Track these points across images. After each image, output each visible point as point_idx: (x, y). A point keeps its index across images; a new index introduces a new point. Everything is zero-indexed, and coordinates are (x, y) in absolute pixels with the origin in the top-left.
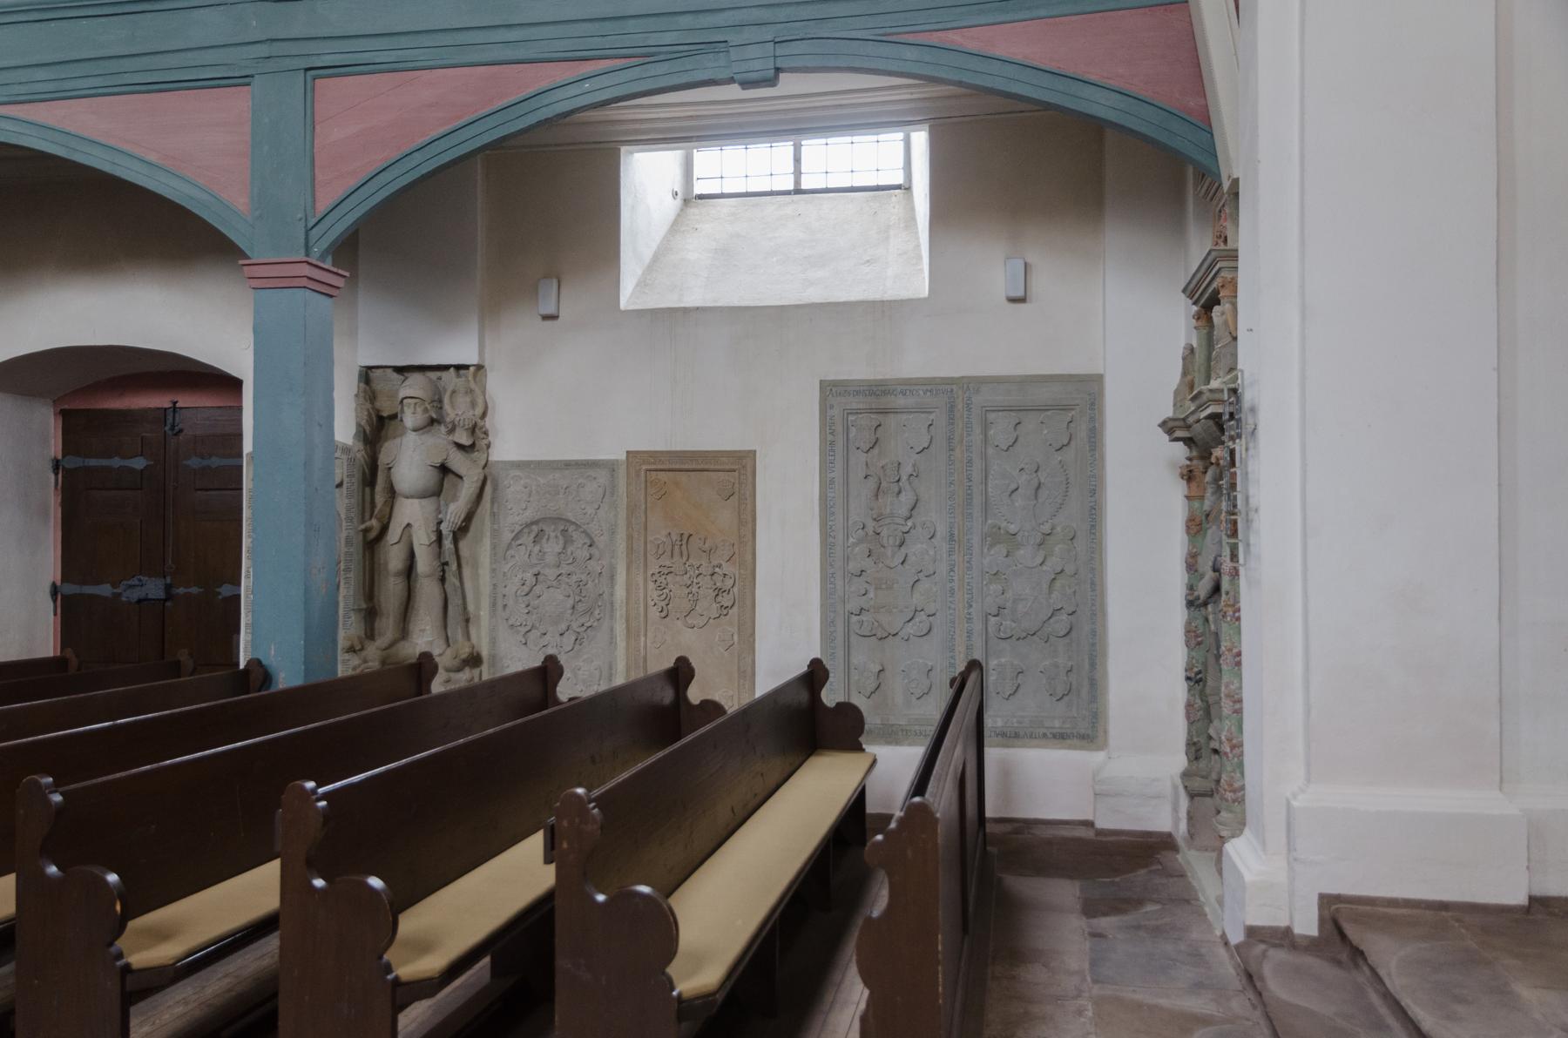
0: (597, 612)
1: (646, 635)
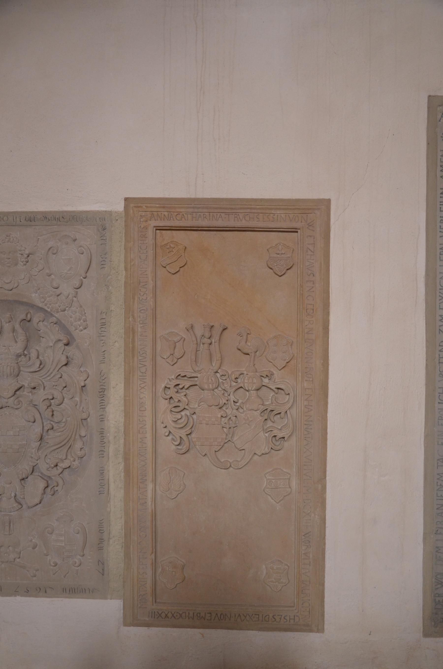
0: (79, 445)
1: (155, 480)
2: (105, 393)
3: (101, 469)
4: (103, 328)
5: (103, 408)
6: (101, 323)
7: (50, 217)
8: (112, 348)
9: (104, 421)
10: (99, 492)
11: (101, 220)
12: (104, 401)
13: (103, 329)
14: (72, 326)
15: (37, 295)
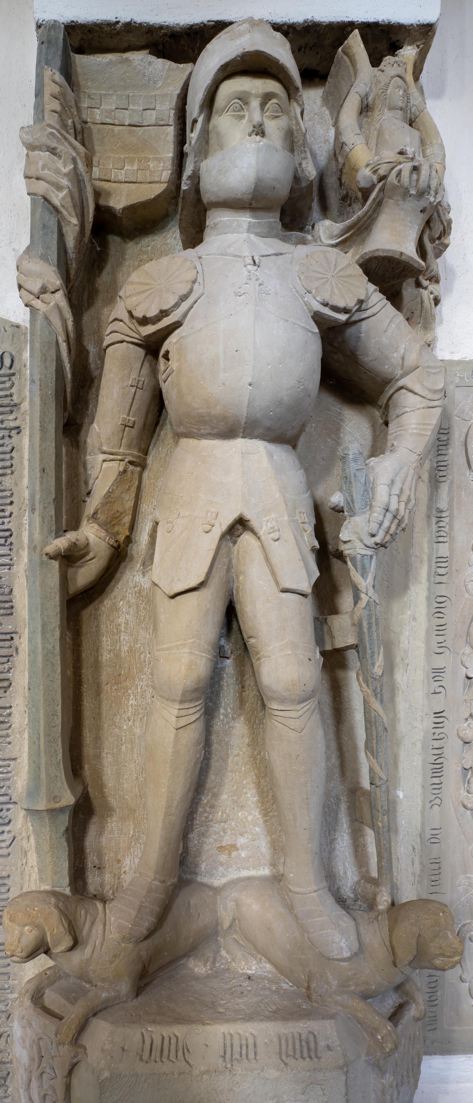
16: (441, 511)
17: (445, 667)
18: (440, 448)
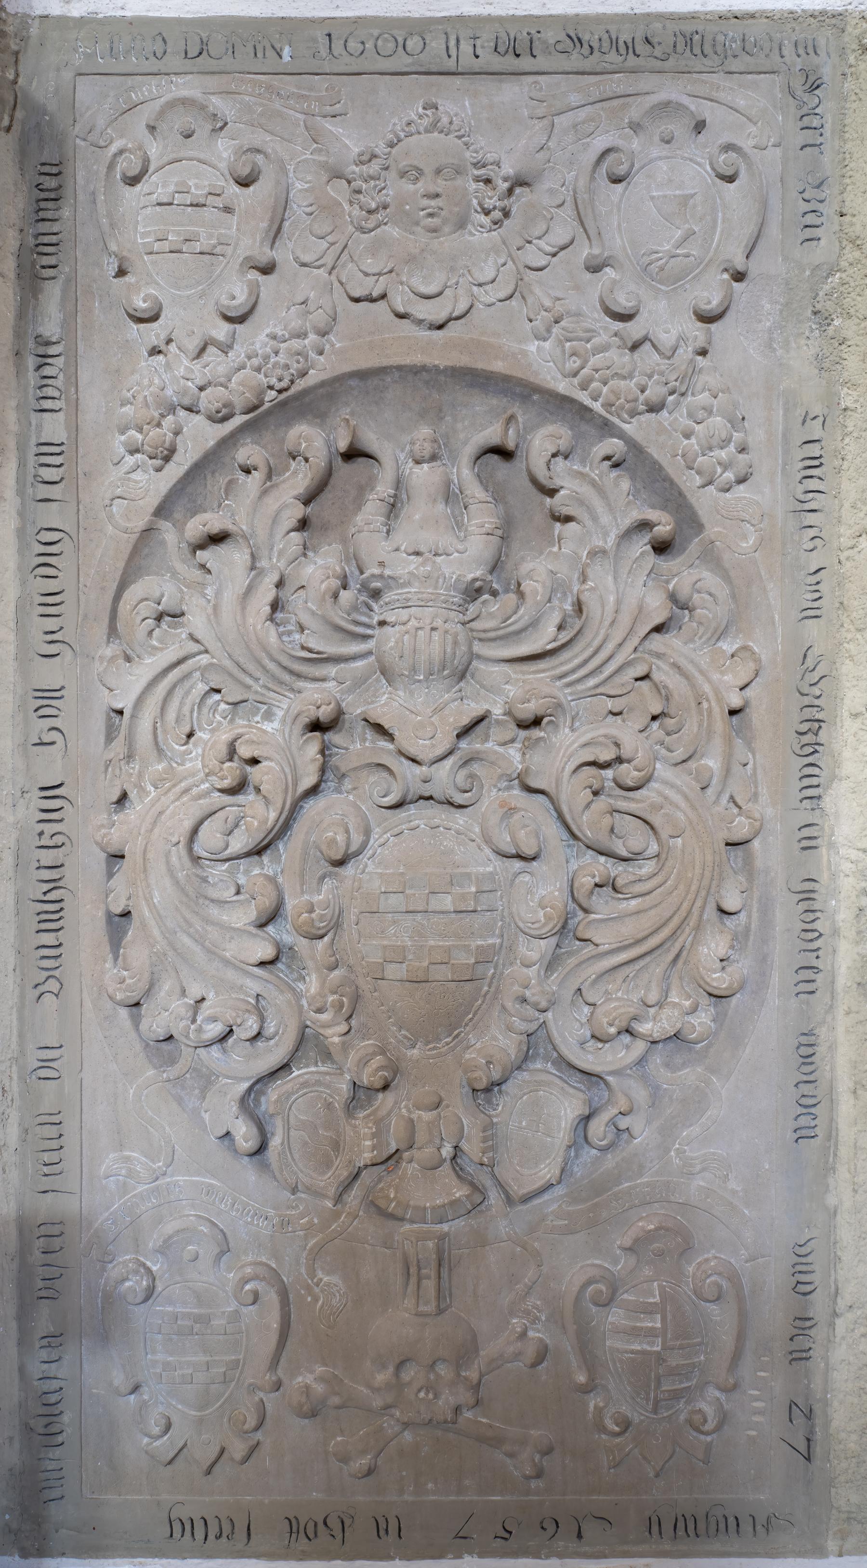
2: (823, 737)
3: (804, 1040)
4: (811, 477)
5: (811, 798)
6: (803, 459)
7: (597, 37)
8: (848, 559)
9: (816, 847)
10: (795, 1131)
11: (801, 51)
12: (816, 771)
13: (813, 484)
14: (692, 469)
15: (547, 345)
16: (48, 343)
17: (63, 688)
18: (43, 205)
